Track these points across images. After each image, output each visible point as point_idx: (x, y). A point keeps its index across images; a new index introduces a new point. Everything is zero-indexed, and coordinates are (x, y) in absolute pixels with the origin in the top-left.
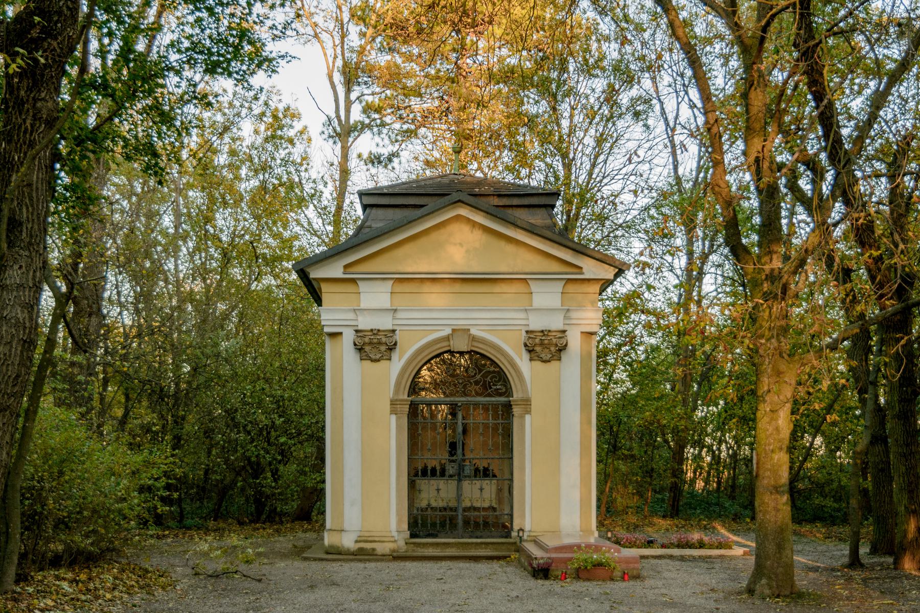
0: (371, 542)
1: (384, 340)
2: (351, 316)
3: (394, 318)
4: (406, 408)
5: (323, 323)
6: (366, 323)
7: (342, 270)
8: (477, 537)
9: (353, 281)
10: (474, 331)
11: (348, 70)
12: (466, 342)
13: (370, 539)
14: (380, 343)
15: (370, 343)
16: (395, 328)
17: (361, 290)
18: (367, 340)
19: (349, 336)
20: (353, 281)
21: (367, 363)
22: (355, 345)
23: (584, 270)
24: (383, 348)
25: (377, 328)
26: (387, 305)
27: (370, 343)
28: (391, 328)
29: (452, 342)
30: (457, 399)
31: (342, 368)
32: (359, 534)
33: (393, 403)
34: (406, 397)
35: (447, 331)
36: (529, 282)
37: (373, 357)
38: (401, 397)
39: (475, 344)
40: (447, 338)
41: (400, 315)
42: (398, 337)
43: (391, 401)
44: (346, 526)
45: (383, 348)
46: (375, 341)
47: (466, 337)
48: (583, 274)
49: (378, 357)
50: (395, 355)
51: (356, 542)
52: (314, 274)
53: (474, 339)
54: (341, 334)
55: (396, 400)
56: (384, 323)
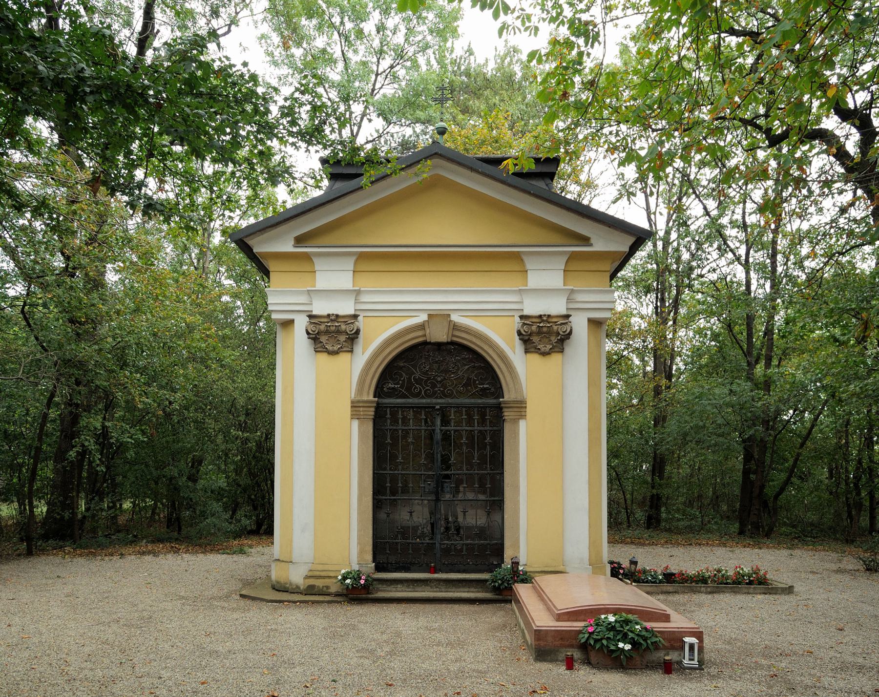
0: (324, 577)
1: (343, 327)
2: (303, 299)
3: (357, 302)
4: (371, 412)
5: (270, 308)
6: (321, 308)
7: (293, 243)
8: (459, 572)
9: (307, 257)
10: (455, 318)
11: (141, 101)
12: (446, 330)
13: (323, 574)
14: (339, 332)
15: (327, 332)
16: (357, 313)
17: (317, 268)
18: (322, 327)
19: (301, 323)
20: (307, 257)
21: (323, 357)
22: (308, 333)
23: (592, 241)
24: (342, 338)
25: (335, 313)
26: (349, 286)
27: (327, 332)
28: (352, 312)
29: (428, 331)
30: (434, 401)
31: (293, 360)
32: (310, 566)
33: (355, 405)
34: (371, 398)
35: (423, 317)
36: (525, 258)
37: (329, 347)
38: (365, 398)
39: (457, 333)
40: (422, 326)
41: (365, 298)
42: (361, 323)
43: (352, 402)
44: (295, 557)
45: (342, 338)
46: (333, 328)
47: (446, 324)
48: (591, 245)
49: (335, 348)
50: (358, 348)
51: (307, 577)
52: (260, 247)
53: (455, 327)
54: (292, 322)
55: (359, 402)
56: (345, 308)
